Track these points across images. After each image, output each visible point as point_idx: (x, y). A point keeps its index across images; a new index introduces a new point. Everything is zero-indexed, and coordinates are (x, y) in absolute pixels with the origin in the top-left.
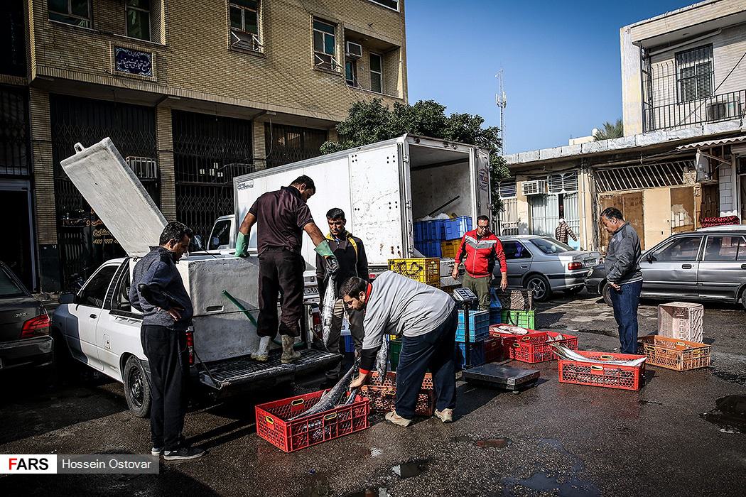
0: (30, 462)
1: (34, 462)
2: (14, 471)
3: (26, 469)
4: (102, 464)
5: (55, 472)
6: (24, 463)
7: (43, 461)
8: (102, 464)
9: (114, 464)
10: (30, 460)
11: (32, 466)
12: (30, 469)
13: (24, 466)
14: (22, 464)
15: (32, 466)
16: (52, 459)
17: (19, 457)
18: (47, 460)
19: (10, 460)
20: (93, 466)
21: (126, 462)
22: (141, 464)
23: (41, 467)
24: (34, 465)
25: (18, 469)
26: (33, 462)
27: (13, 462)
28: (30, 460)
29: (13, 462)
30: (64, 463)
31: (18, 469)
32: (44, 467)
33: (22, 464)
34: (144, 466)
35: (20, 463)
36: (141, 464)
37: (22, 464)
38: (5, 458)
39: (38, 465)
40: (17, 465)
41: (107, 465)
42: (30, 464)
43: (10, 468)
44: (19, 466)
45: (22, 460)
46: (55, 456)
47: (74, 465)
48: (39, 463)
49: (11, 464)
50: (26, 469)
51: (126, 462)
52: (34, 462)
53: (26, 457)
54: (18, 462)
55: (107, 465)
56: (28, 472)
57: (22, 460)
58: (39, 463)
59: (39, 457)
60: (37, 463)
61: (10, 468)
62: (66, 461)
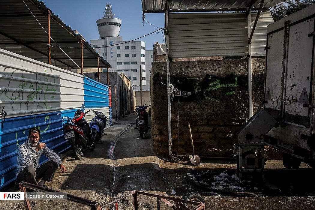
0: (13, 195)
1: (14, 195)
2: (6, 199)
3: (11, 198)
4: (43, 196)
5: (23, 199)
6: (10, 196)
7: (18, 195)
8: (43, 196)
9: (48, 196)
10: (13, 194)
11: (14, 197)
12: (13, 198)
13: (10, 197)
14: (9, 196)
15: (14, 197)
16: (22, 194)
17: (8, 193)
18: (20, 195)
19: (4, 194)
20: (39, 197)
21: (53, 195)
22: (59, 196)
23: (17, 197)
24: (14, 196)
25: (8, 198)
26: (14, 195)
27: (5, 195)
28: (13, 194)
29: (5, 195)
30: (27, 196)
31: (8, 198)
32: (19, 197)
33: (9, 196)
34: (61, 197)
35: (9, 196)
36: (59, 196)
37: (9, 196)
38: (3, 193)
39: (16, 196)
40: (7, 196)
41: (45, 196)
42: (13, 196)
43: (4, 198)
44: (8, 197)
45: (9, 194)
46: (23, 193)
47: (31, 197)
48: (16, 195)
49: (5, 196)
50: (11, 198)
51: (53, 195)
52: (14, 195)
53: (11, 193)
54: (7, 195)
55: (45, 196)
56: (12, 199)
57: (9, 194)
58: (16, 195)
59: (16, 193)
60: (15, 196)
61: (4, 198)
62: (28, 195)
